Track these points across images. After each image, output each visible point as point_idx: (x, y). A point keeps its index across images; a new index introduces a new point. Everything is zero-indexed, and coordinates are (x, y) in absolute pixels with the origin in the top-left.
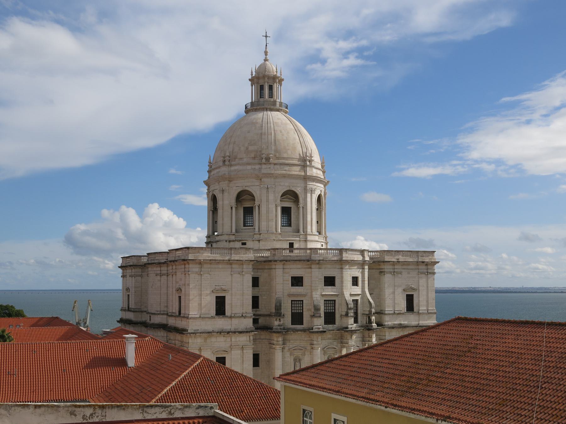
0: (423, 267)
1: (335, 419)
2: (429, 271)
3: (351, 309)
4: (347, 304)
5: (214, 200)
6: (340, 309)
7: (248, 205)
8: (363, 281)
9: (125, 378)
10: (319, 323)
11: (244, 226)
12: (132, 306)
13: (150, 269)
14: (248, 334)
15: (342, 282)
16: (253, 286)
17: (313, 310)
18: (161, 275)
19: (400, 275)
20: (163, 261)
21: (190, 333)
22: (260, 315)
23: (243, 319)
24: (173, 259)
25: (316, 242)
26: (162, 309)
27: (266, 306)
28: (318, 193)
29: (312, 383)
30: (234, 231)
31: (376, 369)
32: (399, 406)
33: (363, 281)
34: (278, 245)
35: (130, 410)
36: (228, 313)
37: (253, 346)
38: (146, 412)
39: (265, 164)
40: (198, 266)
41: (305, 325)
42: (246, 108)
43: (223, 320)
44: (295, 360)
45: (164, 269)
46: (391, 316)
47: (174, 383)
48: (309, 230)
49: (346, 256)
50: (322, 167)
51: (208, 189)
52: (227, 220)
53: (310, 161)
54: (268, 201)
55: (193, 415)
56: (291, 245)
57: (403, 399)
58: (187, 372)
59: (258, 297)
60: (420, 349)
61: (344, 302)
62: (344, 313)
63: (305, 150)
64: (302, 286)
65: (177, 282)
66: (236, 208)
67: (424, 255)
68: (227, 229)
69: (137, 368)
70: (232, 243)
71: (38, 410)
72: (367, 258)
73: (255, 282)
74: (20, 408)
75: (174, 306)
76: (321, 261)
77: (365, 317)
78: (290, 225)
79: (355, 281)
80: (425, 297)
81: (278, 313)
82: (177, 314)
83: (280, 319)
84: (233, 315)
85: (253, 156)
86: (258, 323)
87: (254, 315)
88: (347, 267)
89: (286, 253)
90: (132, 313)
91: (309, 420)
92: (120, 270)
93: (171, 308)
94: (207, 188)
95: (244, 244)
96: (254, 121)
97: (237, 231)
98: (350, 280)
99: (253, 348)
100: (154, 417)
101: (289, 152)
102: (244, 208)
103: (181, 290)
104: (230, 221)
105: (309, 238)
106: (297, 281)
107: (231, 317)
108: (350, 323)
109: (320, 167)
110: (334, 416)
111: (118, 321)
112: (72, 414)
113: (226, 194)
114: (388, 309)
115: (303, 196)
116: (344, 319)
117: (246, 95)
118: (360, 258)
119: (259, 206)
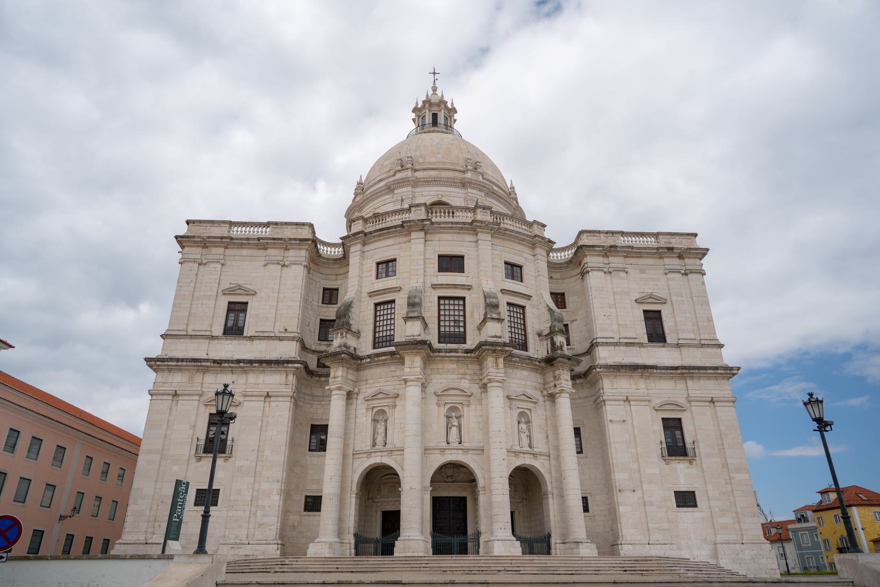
0: (673, 262)
6: (476, 315)
19: (622, 274)
40: (199, 250)
43: (235, 342)
44: (375, 421)
46: (612, 348)
67: (673, 240)
79: (514, 270)
83: (342, 334)
84: (257, 334)
85: (387, 169)
114: (600, 334)
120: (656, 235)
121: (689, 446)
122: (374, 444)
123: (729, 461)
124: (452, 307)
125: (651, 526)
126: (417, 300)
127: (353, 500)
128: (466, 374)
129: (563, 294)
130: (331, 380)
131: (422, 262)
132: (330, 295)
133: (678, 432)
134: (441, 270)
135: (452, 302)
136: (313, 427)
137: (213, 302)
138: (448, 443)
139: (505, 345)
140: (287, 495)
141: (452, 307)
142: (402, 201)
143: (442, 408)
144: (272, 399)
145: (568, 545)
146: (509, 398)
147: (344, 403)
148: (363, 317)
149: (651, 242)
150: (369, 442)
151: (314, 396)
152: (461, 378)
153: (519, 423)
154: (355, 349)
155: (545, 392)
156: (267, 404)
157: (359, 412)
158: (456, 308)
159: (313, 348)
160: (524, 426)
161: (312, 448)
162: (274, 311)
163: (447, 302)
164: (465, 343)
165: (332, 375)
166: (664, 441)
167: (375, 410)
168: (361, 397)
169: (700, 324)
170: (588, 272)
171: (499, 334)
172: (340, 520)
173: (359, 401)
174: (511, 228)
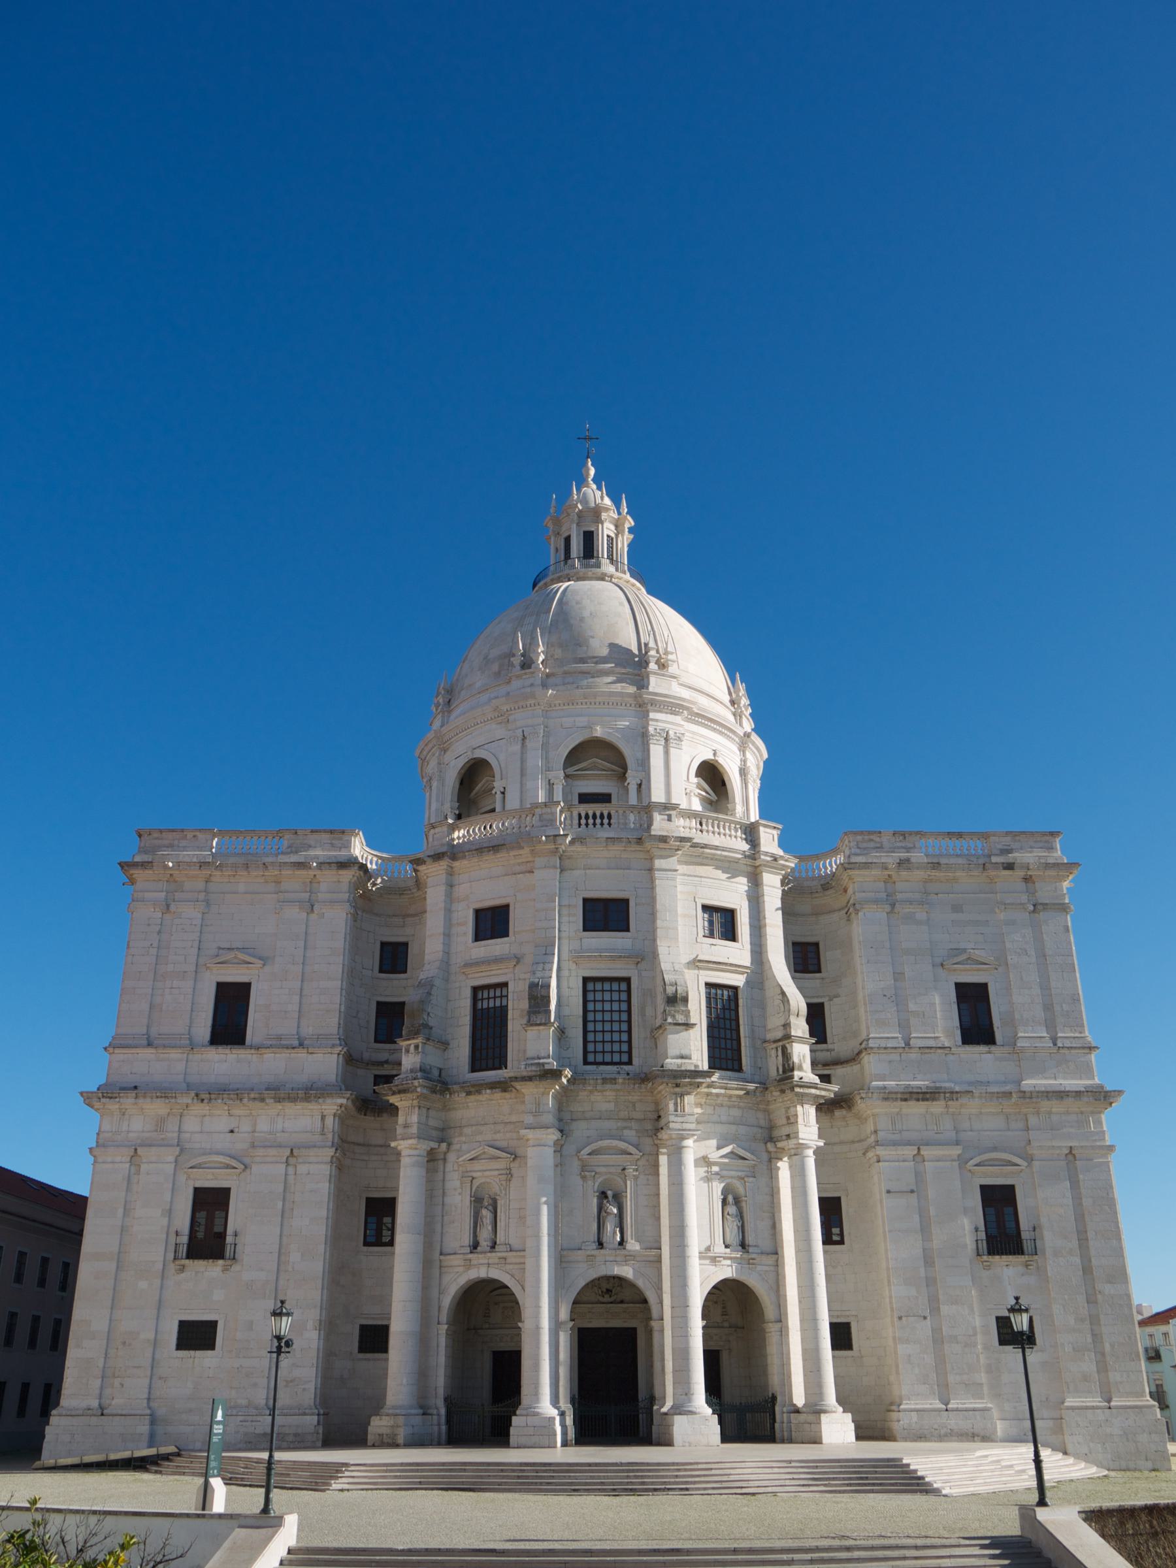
6: (649, 1011)
14: (313, 1107)
15: (653, 915)
23: (301, 1055)
39: (518, 677)
46: (895, 1057)
50: (733, 702)
53: (662, 666)
77: (773, 1053)
83: (417, 1047)
88: (671, 863)
106: (492, 922)
108: (672, 1051)
115: (639, 755)
119: (503, 793)
120: (985, 836)
121: (1025, 1235)
122: (475, 1246)
123: (1094, 1262)
124: (607, 996)
125: (951, 1379)
126: (543, 993)
127: (443, 1341)
128: (631, 1119)
129: (817, 945)
130: (399, 1130)
132: (394, 957)
133: (1008, 1210)
134: (589, 925)
135: (607, 986)
136: (370, 1202)
137: (191, 983)
138: (601, 1245)
139: (696, 1073)
140: (329, 1328)
141: (607, 996)
142: (524, 738)
143: (590, 1183)
144: (300, 1160)
145: (802, 1417)
146: (704, 1161)
147: (423, 1172)
149: (977, 846)
150: (467, 1240)
151: (369, 1145)
152: (625, 1128)
153: (724, 1202)
154: (441, 1070)
155: (769, 1145)
156: (291, 1170)
157: (449, 1185)
158: (615, 996)
159: (366, 1056)
160: (732, 1209)
161: (369, 1240)
162: (296, 998)
163: (599, 986)
164: (630, 1063)
165: (401, 1119)
166: (982, 1228)
167: (476, 1183)
168: (451, 1157)
169: (1057, 1008)
170: (857, 912)
171: (684, 1052)
172: (422, 1374)
173: (449, 1167)
174: (715, 840)
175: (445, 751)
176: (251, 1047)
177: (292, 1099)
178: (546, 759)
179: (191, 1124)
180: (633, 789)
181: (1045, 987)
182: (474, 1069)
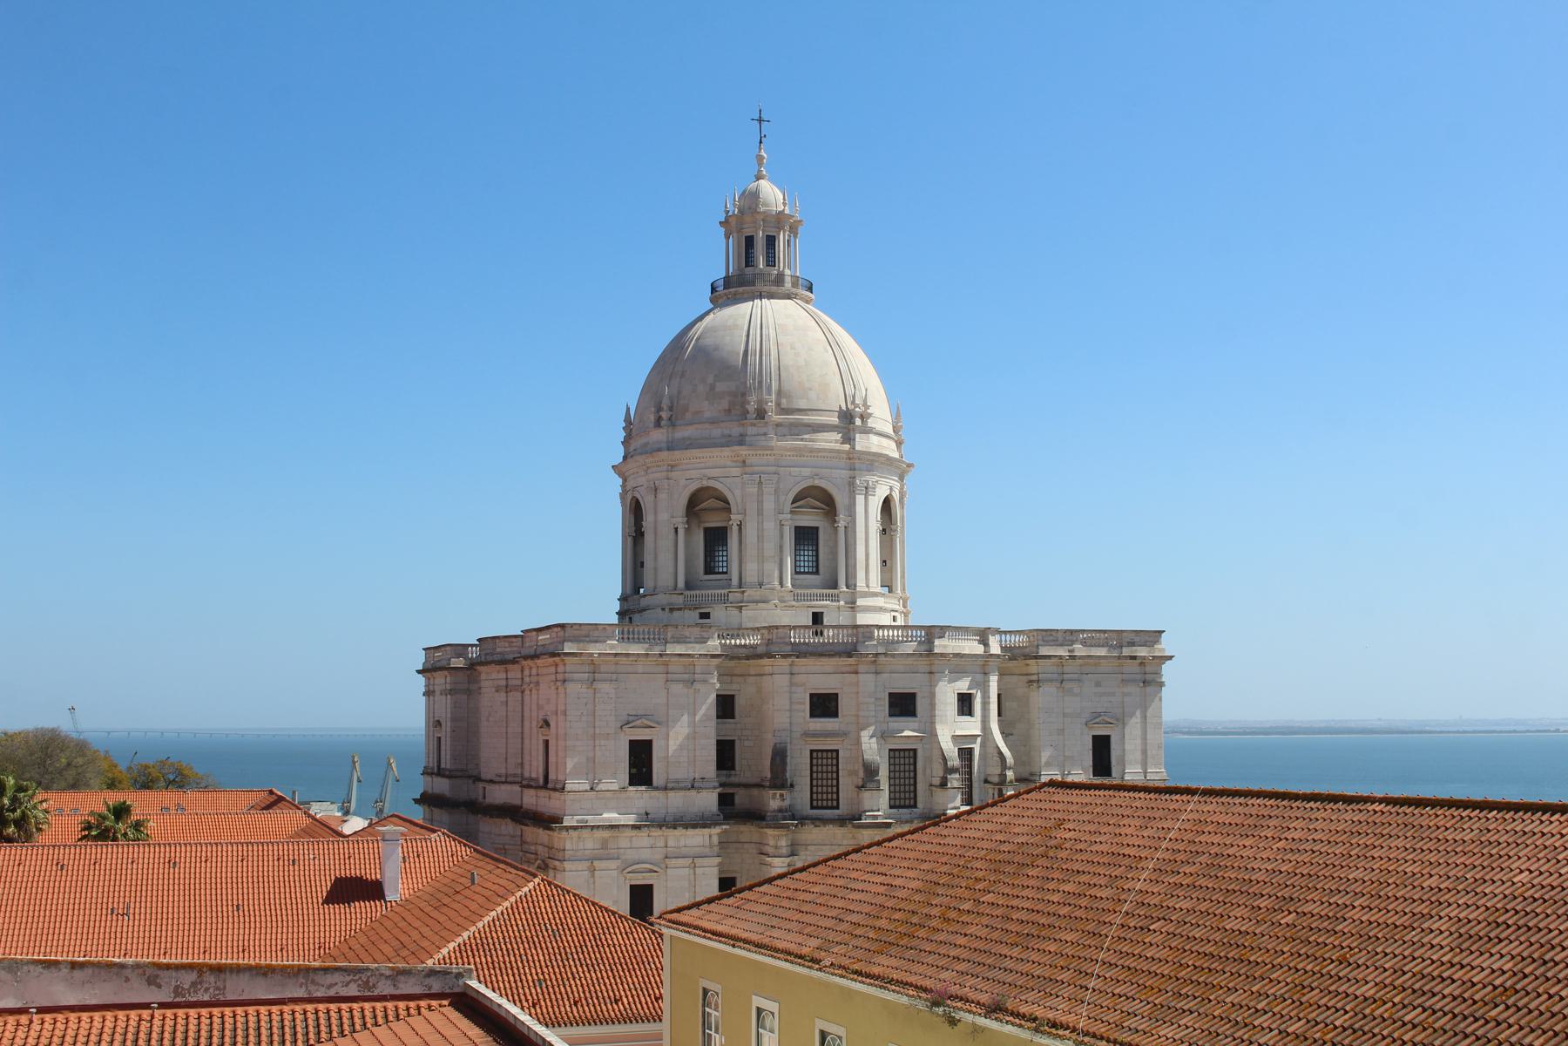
1: (758, 1009)
2: (1149, 677)
3: (953, 770)
4: (945, 759)
5: (635, 512)
7: (714, 522)
8: (985, 704)
9: (376, 925)
10: (878, 804)
11: (706, 573)
12: (446, 763)
13: (483, 676)
14: (706, 831)
15: (932, 706)
16: (718, 717)
17: (861, 774)
18: (508, 689)
20: (511, 657)
21: (567, 828)
22: (739, 785)
23: (693, 793)
24: (532, 652)
25: (879, 612)
26: (511, 771)
27: (753, 762)
28: (881, 492)
29: (719, 928)
30: (681, 584)
31: (853, 896)
32: (868, 976)
33: (985, 704)
34: (785, 617)
35: (278, 977)
36: (658, 778)
37: (718, 860)
38: (313, 982)
41: (844, 809)
42: (713, 289)
45: (514, 672)
47: (465, 935)
48: (861, 584)
49: (940, 645)
51: (623, 486)
52: (665, 558)
54: (760, 512)
55: (418, 990)
56: (817, 618)
57: (883, 960)
58: (499, 909)
59: (732, 743)
60: (953, 851)
61: (936, 753)
62: (937, 781)
63: (850, 391)
64: (835, 715)
65: (539, 707)
66: (687, 531)
68: (665, 579)
69: (405, 904)
70: (676, 614)
71: (77, 974)
72: (995, 649)
73: (726, 707)
74: (39, 969)
75: (534, 764)
76: (882, 658)
78: (817, 573)
79: (965, 704)
80: (1139, 741)
81: (779, 780)
82: (541, 781)
86: (732, 803)
87: (721, 785)
89: (808, 637)
90: (446, 781)
91: (714, 1013)
92: (421, 680)
93: (527, 767)
94: (620, 481)
95: (705, 616)
96: (730, 322)
97: (689, 586)
98: (954, 700)
99: (720, 864)
100: (332, 993)
101: (812, 395)
102: (706, 530)
103: (547, 723)
104: (671, 564)
105: (860, 602)
106: (824, 705)
107: (666, 789)
109: (890, 430)
110: (757, 1001)
111: (416, 801)
112: (152, 981)
113: (662, 496)
115: (847, 501)
116: (940, 795)
117: (716, 260)
118: (980, 649)
119: (740, 526)
131: (872, 707)
148: (799, 766)
164: (915, 806)
175: (672, 467)
176: (657, 789)
177: (694, 826)
178: (777, 501)
179: (624, 843)
180: (841, 531)
181: (1144, 739)
182: (812, 807)
